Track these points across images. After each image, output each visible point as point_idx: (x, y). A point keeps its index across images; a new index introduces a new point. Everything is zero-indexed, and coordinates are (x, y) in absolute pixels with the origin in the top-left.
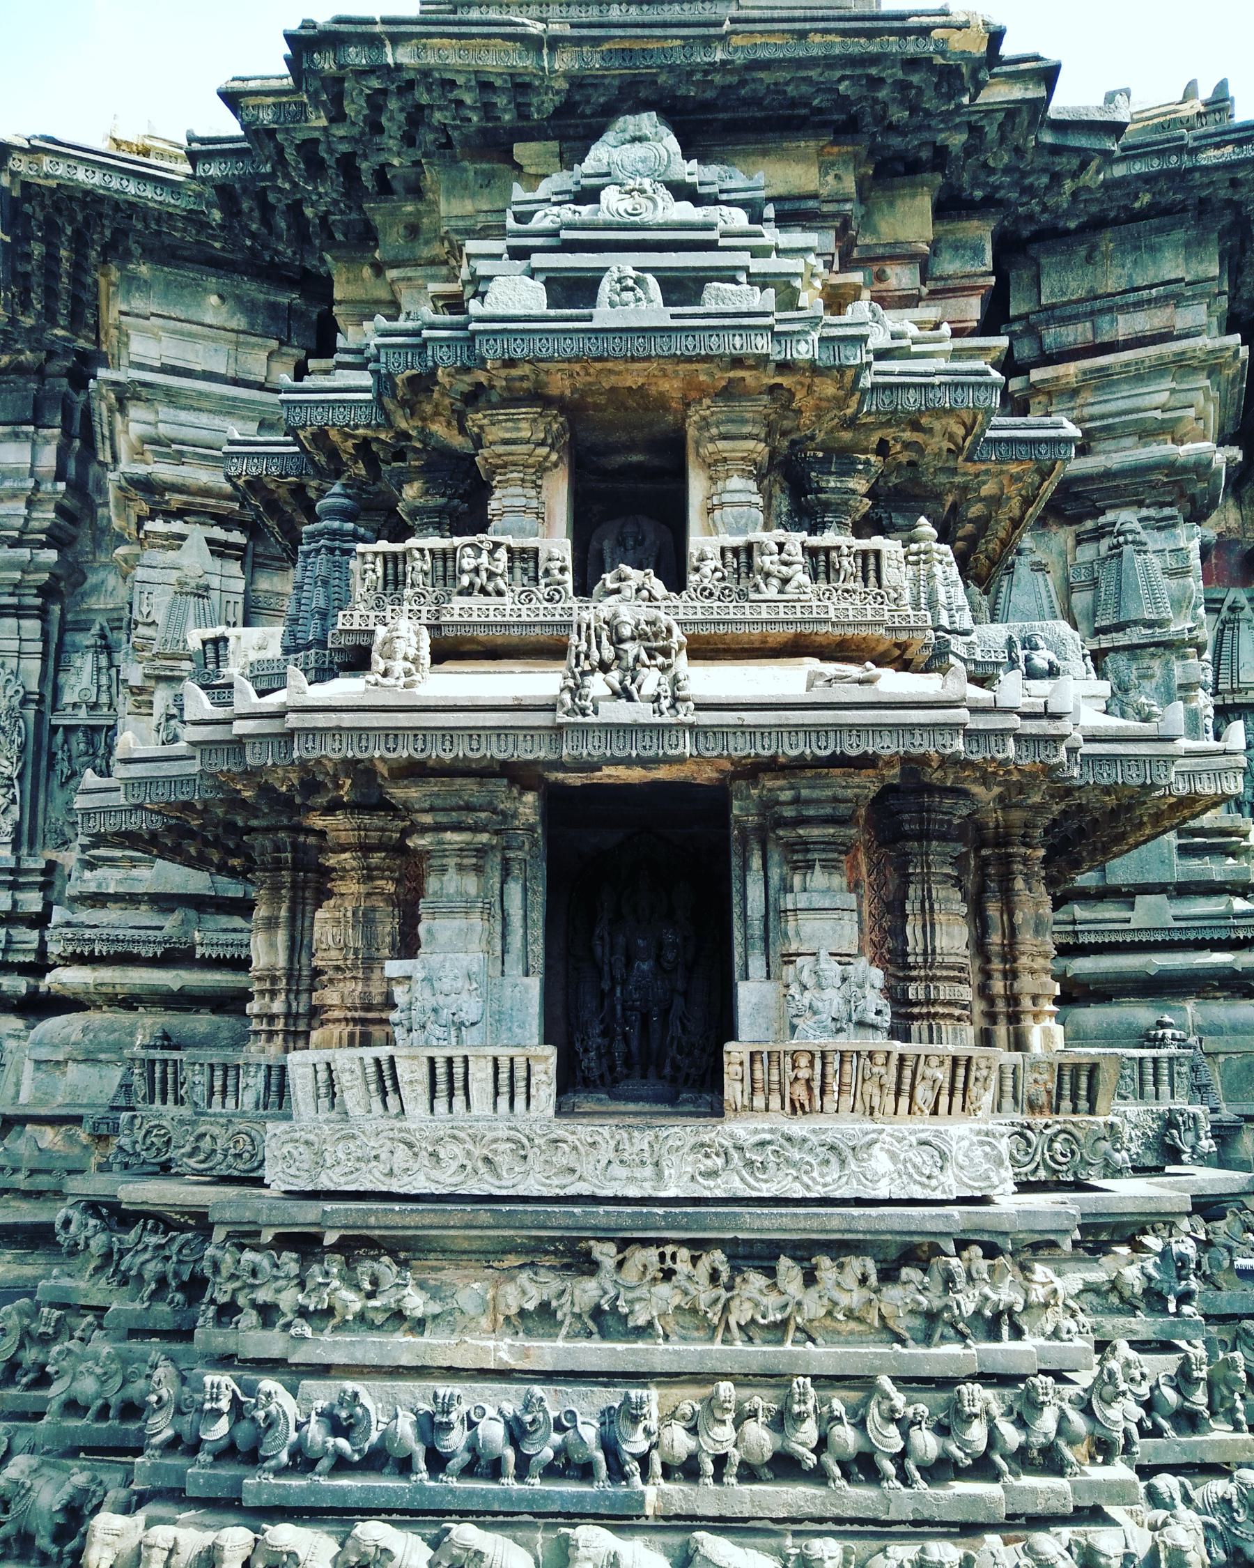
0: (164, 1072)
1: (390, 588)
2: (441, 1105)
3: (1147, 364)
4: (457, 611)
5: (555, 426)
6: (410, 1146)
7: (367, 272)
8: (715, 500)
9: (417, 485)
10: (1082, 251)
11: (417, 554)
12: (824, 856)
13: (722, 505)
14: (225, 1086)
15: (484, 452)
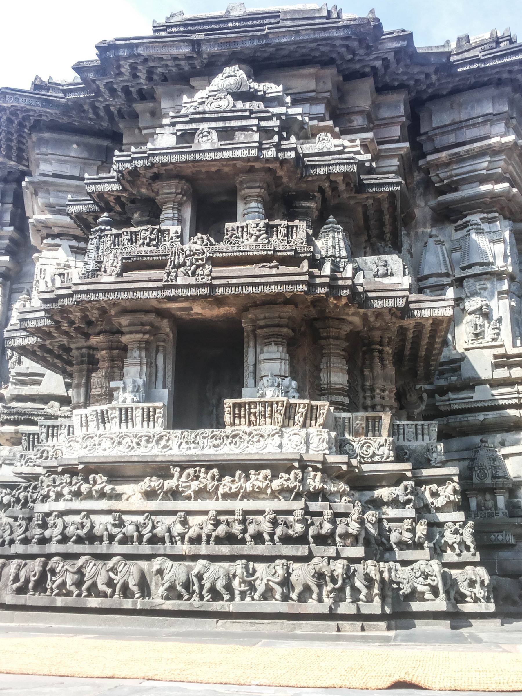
0: (34, 438)
1: (117, 247)
2: (124, 425)
3: (476, 150)
4: (136, 252)
5: (185, 187)
6: (112, 439)
7: (137, 131)
8: (245, 211)
9: (138, 213)
10: (448, 104)
11: (125, 233)
12: (275, 340)
13: (248, 213)
14: (53, 434)
15: (158, 198)
